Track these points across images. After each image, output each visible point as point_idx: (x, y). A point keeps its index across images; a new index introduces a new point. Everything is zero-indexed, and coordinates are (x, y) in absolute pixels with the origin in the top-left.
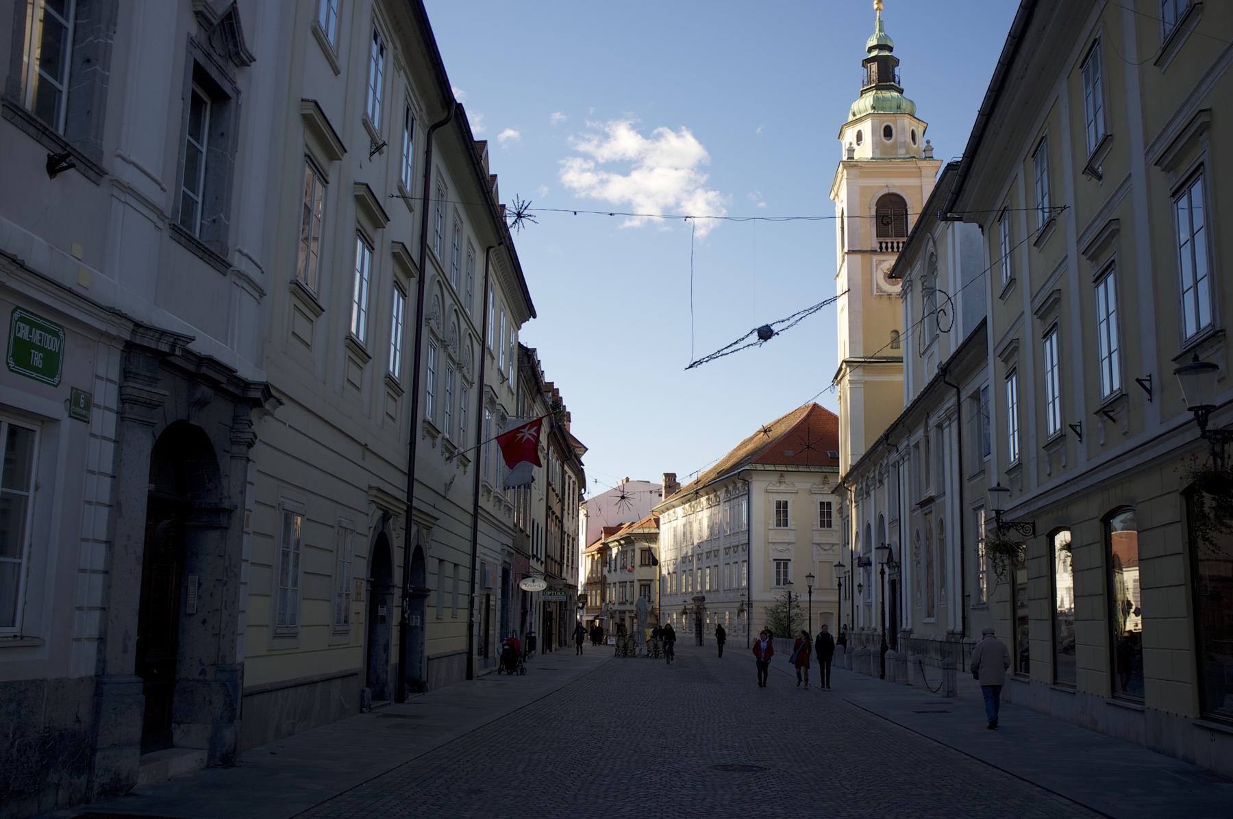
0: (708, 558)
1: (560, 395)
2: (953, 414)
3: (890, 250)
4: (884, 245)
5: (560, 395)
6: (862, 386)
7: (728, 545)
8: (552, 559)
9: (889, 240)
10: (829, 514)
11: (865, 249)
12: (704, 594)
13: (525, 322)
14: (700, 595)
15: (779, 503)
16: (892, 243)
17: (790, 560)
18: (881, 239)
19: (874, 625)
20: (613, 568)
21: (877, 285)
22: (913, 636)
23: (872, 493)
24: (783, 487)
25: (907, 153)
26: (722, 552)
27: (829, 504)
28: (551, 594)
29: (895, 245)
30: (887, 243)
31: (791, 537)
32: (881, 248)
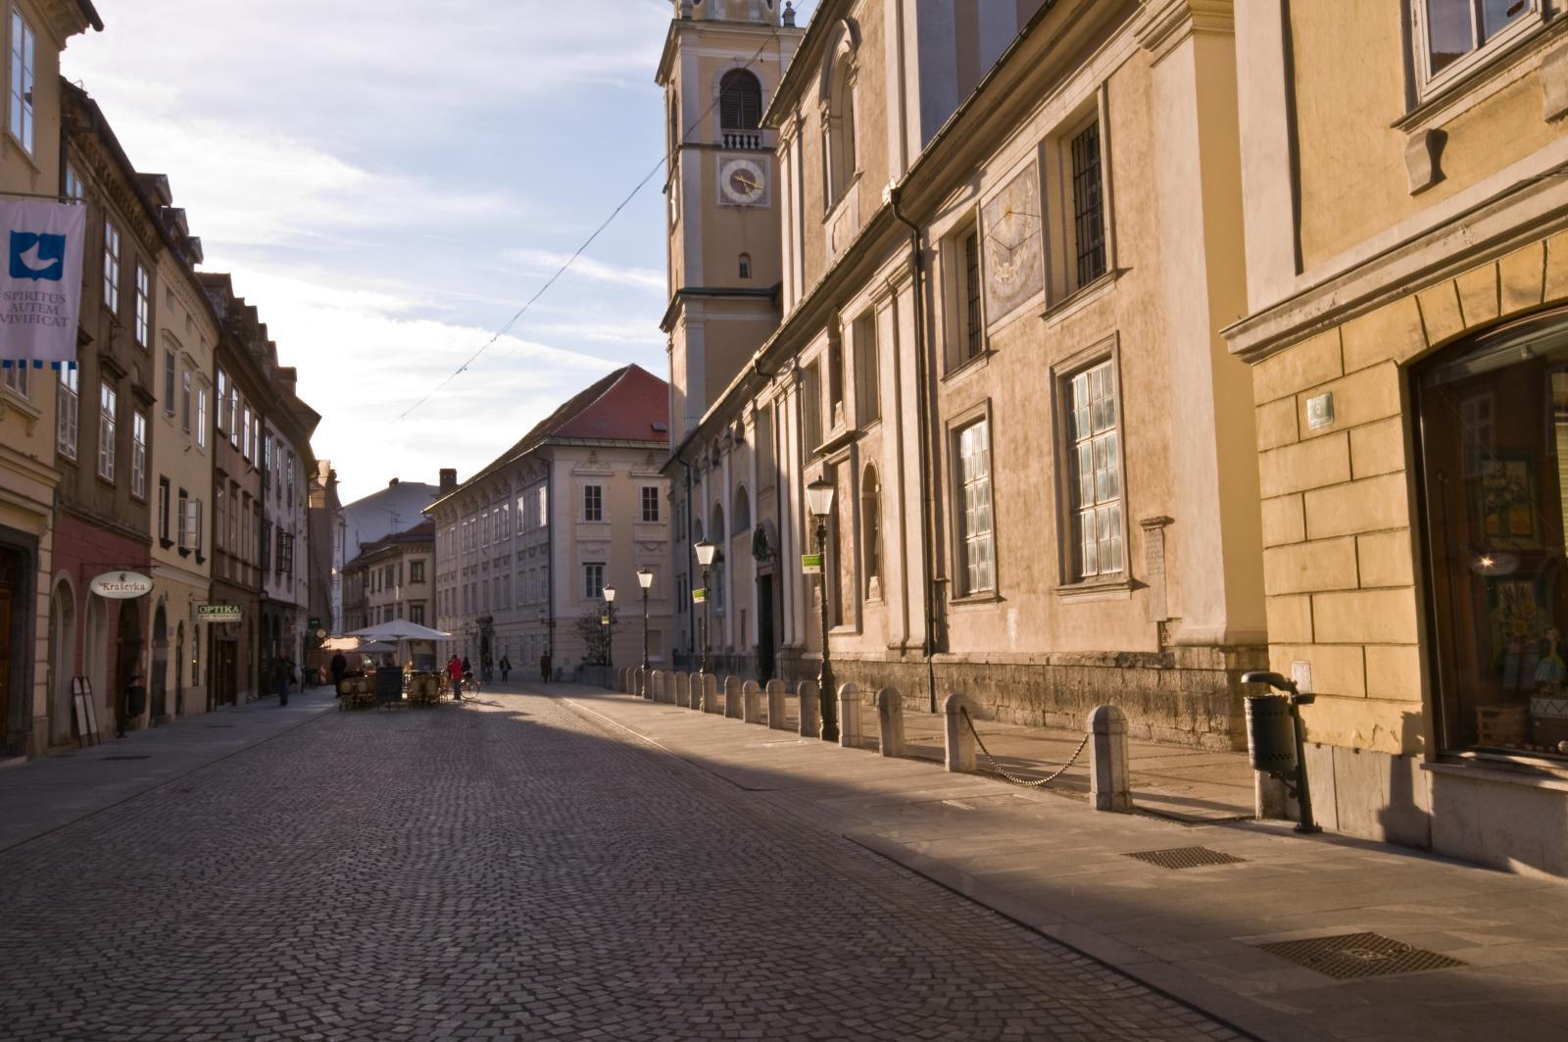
0: (495, 566)
1: (192, 234)
2: (903, 278)
3: (738, 146)
4: (730, 139)
5: (270, 338)
6: (701, 326)
7: (522, 548)
8: (234, 558)
9: (737, 133)
10: (655, 504)
11: (706, 143)
12: (492, 614)
13: (73, 33)
14: (486, 615)
15: (588, 489)
16: (742, 137)
17: (604, 564)
18: (727, 131)
19: (729, 642)
20: (377, 587)
21: (722, 191)
22: (804, 656)
23: (725, 461)
24: (594, 469)
25: (761, 16)
26: (514, 558)
27: (655, 491)
28: (213, 612)
29: (745, 140)
30: (734, 137)
31: (605, 533)
32: (726, 142)
